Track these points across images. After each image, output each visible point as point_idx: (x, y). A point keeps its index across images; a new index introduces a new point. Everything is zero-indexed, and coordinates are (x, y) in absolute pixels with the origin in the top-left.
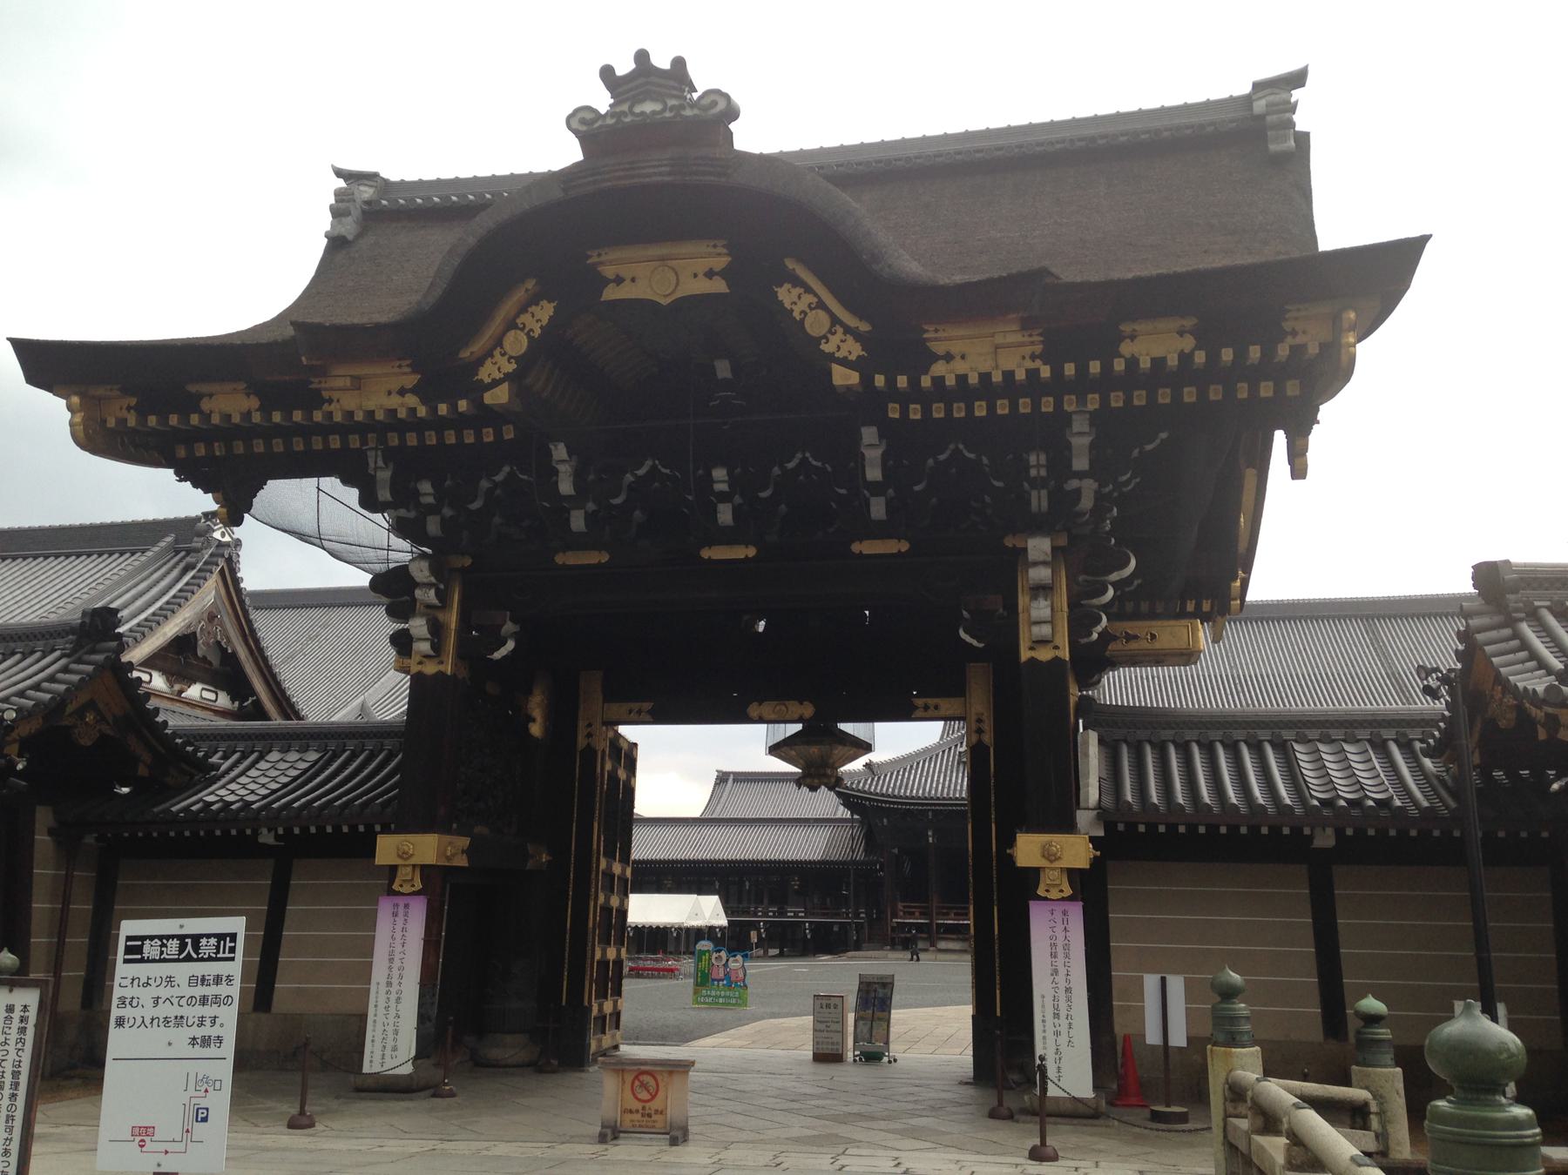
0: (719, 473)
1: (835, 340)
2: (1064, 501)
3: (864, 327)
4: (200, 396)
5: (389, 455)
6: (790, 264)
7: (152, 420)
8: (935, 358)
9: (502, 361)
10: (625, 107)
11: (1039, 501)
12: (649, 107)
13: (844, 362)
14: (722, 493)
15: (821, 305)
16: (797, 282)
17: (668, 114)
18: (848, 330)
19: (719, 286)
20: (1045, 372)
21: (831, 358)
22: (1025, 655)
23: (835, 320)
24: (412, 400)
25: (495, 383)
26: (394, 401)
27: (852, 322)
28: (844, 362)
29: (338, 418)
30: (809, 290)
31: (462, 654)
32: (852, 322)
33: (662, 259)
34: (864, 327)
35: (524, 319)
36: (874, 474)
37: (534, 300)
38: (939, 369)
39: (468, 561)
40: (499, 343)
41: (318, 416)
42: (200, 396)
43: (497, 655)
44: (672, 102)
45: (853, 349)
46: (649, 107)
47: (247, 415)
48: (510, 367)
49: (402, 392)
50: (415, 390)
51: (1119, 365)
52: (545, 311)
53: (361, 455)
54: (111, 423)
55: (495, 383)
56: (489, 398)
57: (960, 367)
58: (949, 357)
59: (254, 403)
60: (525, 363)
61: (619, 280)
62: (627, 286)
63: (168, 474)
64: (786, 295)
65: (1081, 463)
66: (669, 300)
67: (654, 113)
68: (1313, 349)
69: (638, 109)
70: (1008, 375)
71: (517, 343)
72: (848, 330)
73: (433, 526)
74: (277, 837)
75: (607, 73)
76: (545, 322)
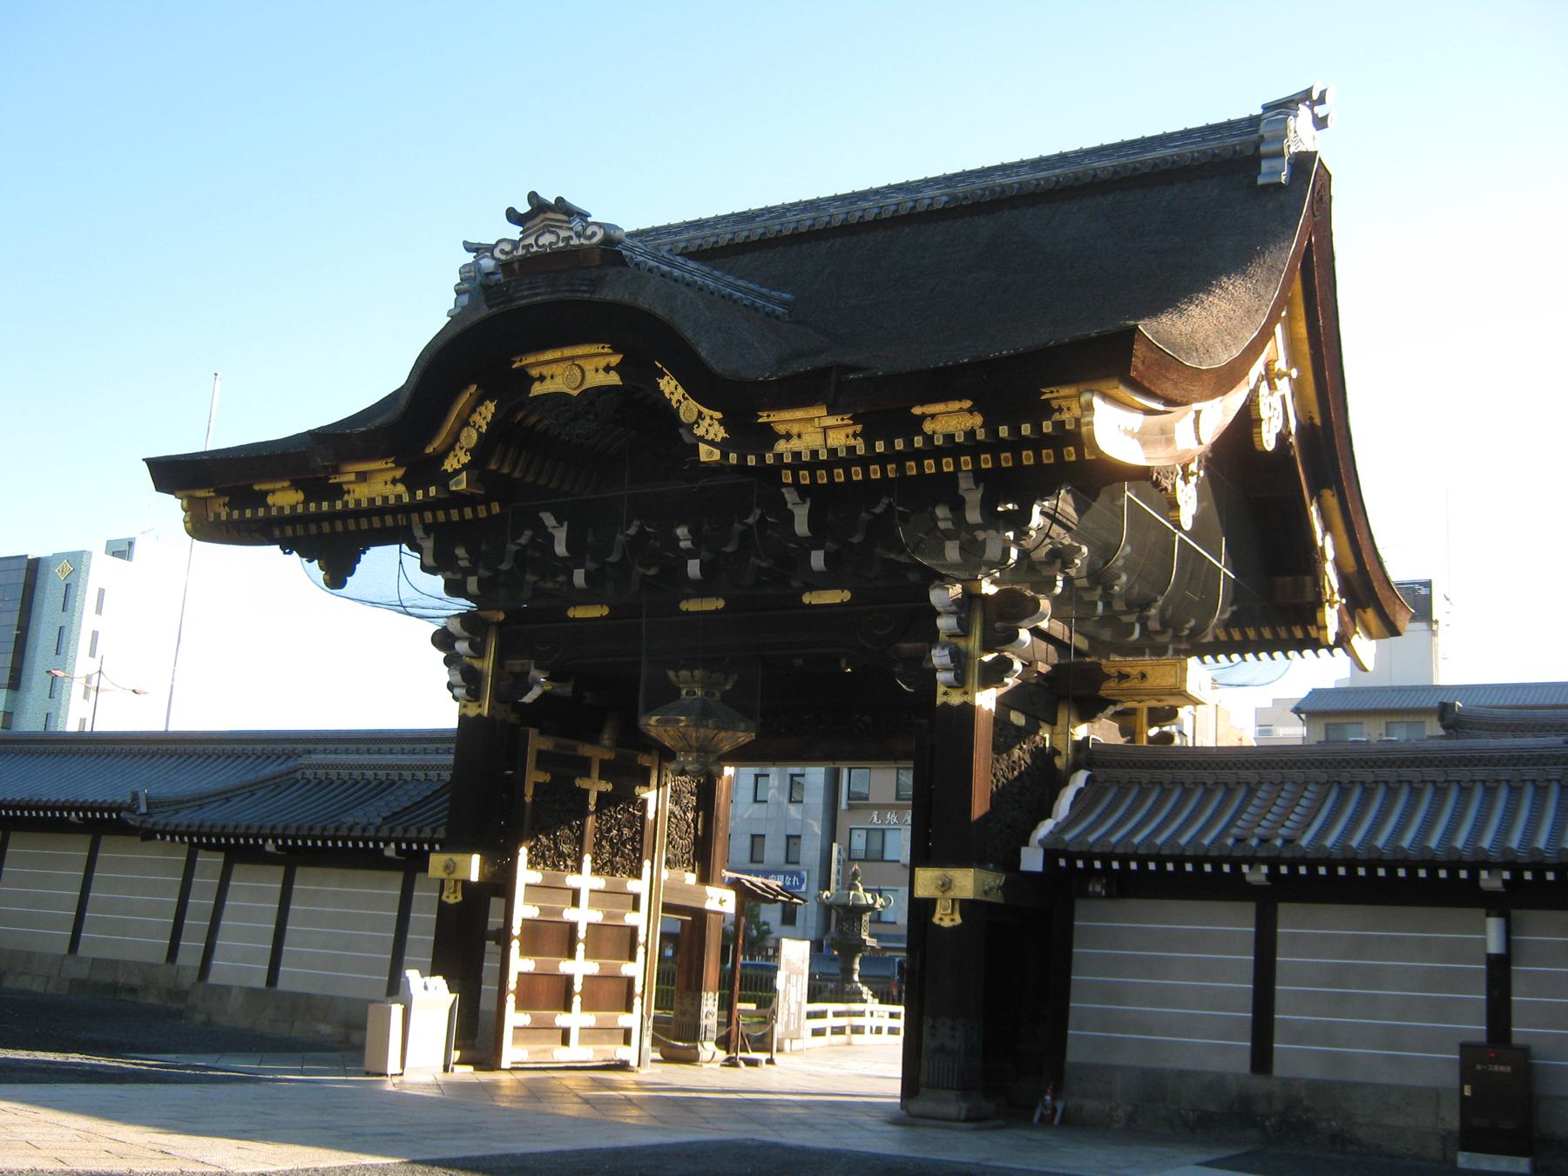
0: (682, 532)
4: (265, 494)
5: (428, 529)
7: (236, 514)
8: (777, 436)
9: (461, 454)
10: (531, 240)
12: (546, 239)
13: (712, 443)
14: (688, 550)
17: (561, 244)
19: (614, 379)
20: (861, 450)
21: (702, 439)
22: (940, 700)
24: (400, 488)
25: (457, 472)
28: (712, 443)
29: (352, 505)
31: (497, 697)
33: (572, 358)
35: (476, 417)
37: (479, 401)
38: (781, 446)
39: (501, 616)
40: (457, 439)
41: (339, 505)
42: (265, 494)
43: (529, 698)
44: (563, 234)
45: (719, 433)
46: (546, 239)
47: (294, 508)
48: (465, 459)
50: (403, 480)
51: (918, 442)
52: (489, 409)
53: (409, 528)
54: (212, 517)
59: (300, 496)
60: (480, 454)
61: (542, 378)
62: (548, 381)
63: (275, 549)
66: (575, 393)
67: (551, 244)
69: (541, 242)
70: (833, 452)
71: (470, 437)
73: (472, 584)
74: (278, 847)
75: (513, 216)
76: (489, 418)
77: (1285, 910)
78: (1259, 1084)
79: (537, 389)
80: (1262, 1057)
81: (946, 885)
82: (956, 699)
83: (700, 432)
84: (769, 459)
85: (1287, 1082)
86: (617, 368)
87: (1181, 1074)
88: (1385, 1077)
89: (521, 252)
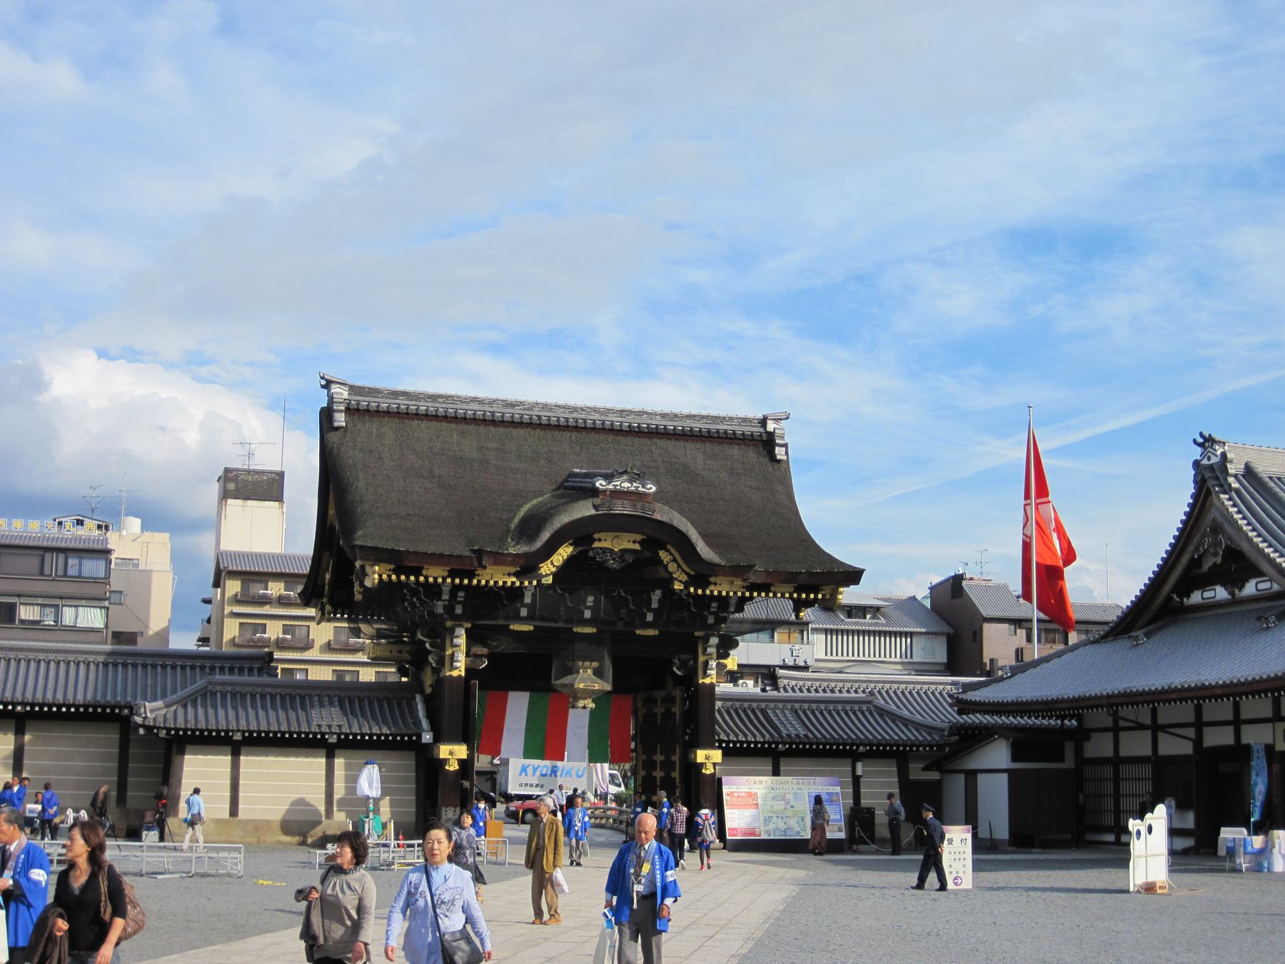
0: (591, 599)
11: (711, 620)
12: (626, 485)
16: (667, 550)
19: (637, 547)
25: (547, 575)
27: (688, 570)
32: (688, 570)
36: (655, 605)
38: (712, 587)
45: (685, 578)
49: (509, 575)
56: (544, 581)
58: (715, 584)
64: (662, 554)
79: (596, 544)
81: (707, 758)
82: (707, 681)
89: (610, 487)
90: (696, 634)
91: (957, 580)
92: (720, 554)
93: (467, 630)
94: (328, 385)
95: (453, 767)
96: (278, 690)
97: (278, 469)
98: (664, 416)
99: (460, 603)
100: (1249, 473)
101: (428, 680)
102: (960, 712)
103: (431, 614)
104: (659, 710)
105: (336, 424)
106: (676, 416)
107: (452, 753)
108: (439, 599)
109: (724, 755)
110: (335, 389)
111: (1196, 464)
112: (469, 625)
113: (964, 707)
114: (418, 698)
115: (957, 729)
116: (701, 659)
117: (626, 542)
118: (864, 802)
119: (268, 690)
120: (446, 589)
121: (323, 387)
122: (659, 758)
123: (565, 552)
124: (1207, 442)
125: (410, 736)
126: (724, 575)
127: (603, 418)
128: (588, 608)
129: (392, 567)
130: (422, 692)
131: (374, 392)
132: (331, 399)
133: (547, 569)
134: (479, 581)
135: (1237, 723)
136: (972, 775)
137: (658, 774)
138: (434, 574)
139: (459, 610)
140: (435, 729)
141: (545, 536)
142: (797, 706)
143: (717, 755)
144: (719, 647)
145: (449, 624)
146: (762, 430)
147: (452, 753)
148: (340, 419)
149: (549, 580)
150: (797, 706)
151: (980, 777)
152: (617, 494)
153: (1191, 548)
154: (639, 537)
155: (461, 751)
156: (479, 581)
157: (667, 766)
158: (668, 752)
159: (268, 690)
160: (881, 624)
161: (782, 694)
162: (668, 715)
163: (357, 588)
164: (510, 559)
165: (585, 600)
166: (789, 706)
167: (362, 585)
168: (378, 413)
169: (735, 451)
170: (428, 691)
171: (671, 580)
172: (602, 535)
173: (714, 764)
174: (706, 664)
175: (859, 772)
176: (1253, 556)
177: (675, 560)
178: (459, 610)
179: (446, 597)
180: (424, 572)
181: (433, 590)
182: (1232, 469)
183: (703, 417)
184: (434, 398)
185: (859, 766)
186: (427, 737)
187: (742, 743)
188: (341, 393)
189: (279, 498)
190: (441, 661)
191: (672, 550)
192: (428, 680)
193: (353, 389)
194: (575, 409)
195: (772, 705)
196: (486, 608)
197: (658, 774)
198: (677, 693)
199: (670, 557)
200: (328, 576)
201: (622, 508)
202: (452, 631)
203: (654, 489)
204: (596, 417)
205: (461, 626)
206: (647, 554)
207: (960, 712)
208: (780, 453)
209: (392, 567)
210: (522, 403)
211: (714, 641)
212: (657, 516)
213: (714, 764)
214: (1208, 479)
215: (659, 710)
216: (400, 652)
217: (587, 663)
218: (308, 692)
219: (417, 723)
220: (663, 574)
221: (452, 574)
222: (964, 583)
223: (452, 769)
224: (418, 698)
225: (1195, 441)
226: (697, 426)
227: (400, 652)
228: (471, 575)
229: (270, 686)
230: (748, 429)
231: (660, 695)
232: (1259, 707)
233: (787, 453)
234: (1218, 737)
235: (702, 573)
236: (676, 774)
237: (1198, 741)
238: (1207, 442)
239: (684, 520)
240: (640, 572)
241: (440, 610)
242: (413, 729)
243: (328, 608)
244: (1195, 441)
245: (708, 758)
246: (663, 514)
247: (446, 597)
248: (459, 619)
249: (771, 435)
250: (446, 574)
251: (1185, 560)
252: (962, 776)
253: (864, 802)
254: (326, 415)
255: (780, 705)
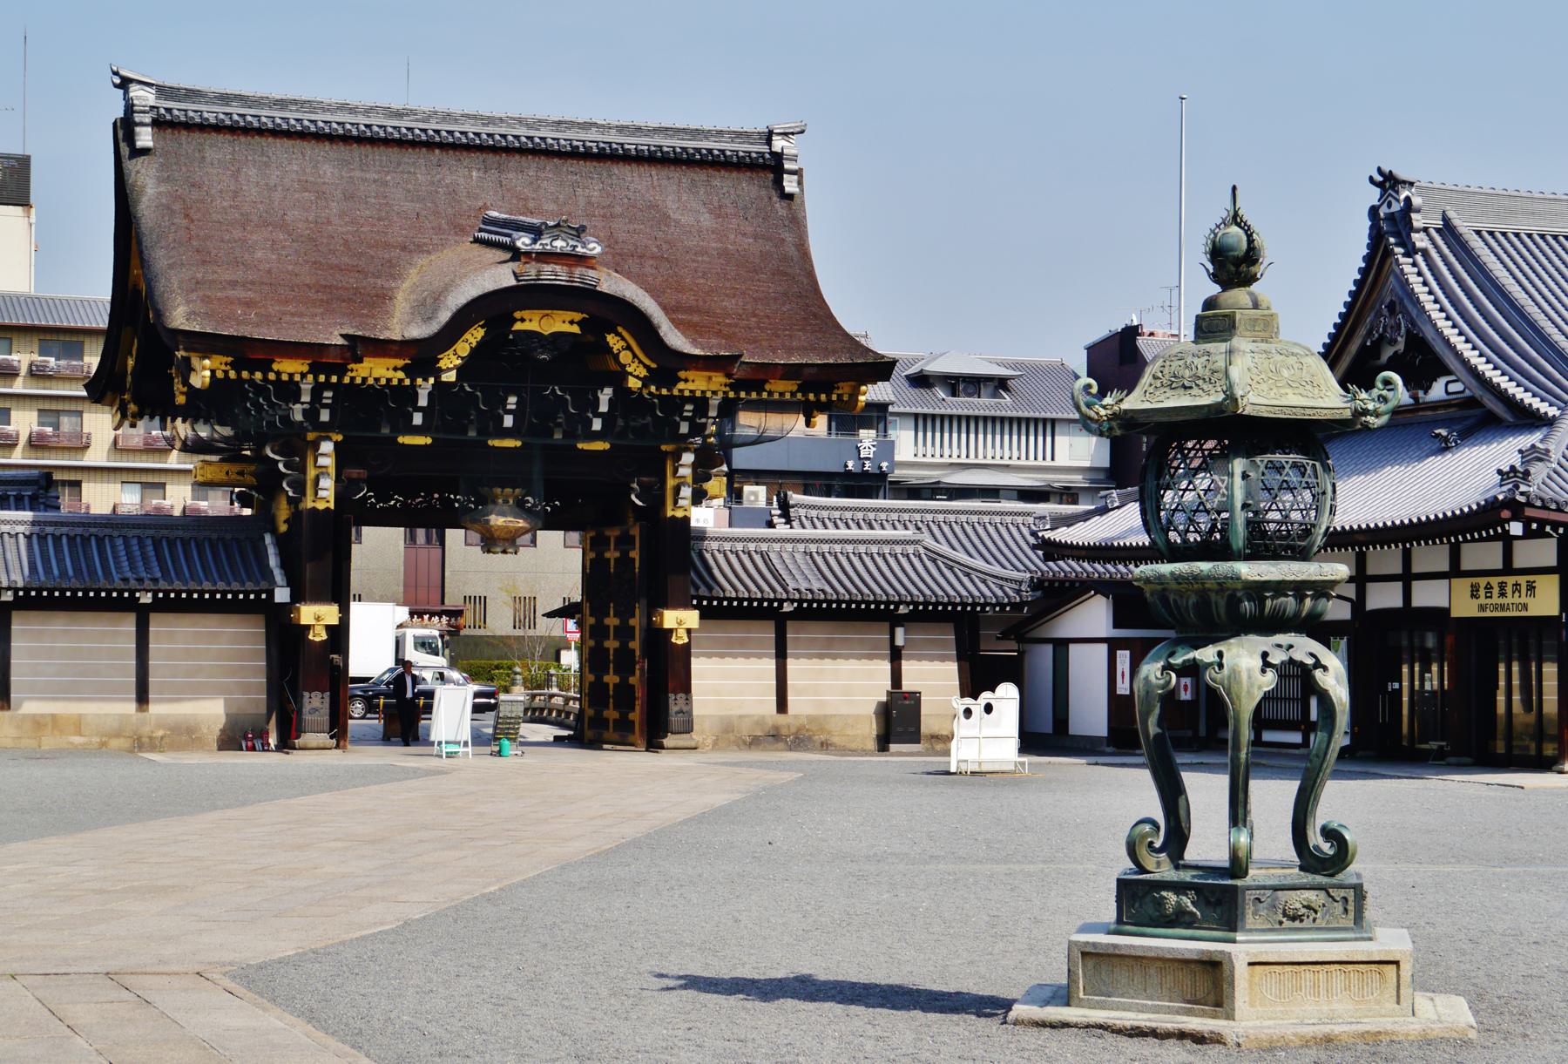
0: (512, 400)
1: (634, 366)
2: (697, 429)
3: (654, 366)
6: (620, 329)
8: (680, 380)
11: (684, 428)
12: (559, 244)
15: (629, 348)
16: (618, 334)
18: (640, 362)
19: (576, 329)
23: (635, 356)
24: (401, 375)
26: (390, 374)
27: (647, 362)
30: (623, 339)
32: (647, 362)
34: (654, 366)
36: (604, 408)
38: (681, 385)
45: (643, 372)
49: (395, 369)
55: (449, 370)
56: (445, 378)
57: (690, 386)
58: (686, 381)
61: (523, 320)
65: (713, 413)
68: (846, 398)
72: (640, 362)
77: (789, 623)
78: (782, 719)
80: (782, 705)
82: (679, 514)
83: (629, 369)
84: (676, 392)
85: (796, 716)
86: (578, 323)
87: (741, 717)
88: (844, 711)
89: (538, 247)
90: (664, 448)
91: (1131, 332)
92: (694, 343)
93: (336, 443)
94: (125, 83)
95: (319, 636)
96: (64, 530)
97: (17, 150)
98: (621, 129)
99: (326, 406)
100: (1448, 230)
101: (283, 512)
102: (1047, 558)
103: (286, 420)
104: (612, 555)
105: (139, 144)
106: (639, 129)
107: (316, 616)
108: (297, 401)
109: (702, 617)
110: (136, 92)
111: (1373, 211)
112: (340, 438)
113: (1053, 550)
114: (268, 539)
115: (1037, 584)
116: (671, 483)
117: (560, 323)
118: (907, 685)
119: (49, 529)
120: (306, 387)
121: (116, 86)
122: (612, 621)
123: (475, 335)
124: (1388, 183)
125: (258, 594)
126: (697, 369)
127: (531, 133)
128: (509, 412)
129: (230, 359)
130: (274, 531)
131: (192, 94)
132: (130, 108)
133: (450, 363)
134: (353, 379)
135: (1407, 578)
136: (1062, 645)
137: (612, 644)
138: (288, 367)
139: (325, 416)
140: (291, 582)
141: (444, 316)
142: (813, 548)
143: (691, 618)
144: (695, 466)
145: (311, 436)
146: (765, 149)
147: (316, 616)
148: (145, 138)
149: (451, 377)
150: (813, 548)
151: (1072, 647)
152: (546, 257)
153: (1362, 331)
154: (578, 316)
155: (330, 614)
156: (353, 379)
157: (625, 632)
158: (625, 613)
159: (49, 529)
160: (1005, 405)
161: (797, 531)
162: (625, 561)
163: (178, 387)
164: (396, 348)
165: (504, 403)
166: (801, 547)
167: (186, 382)
168: (203, 127)
169: (723, 182)
170: (283, 528)
171: (624, 374)
172: (526, 314)
173: (689, 631)
174: (677, 490)
175: (899, 641)
176: (1439, 347)
177: (629, 348)
178: (325, 416)
179: (306, 398)
180: (275, 367)
181: (289, 390)
182: (1418, 220)
183: (678, 130)
184: (282, 104)
185: (900, 632)
186: (282, 595)
187: (730, 600)
188: (144, 97)
189: (20, 198)
190: (300, 487)
191: (625, 334)
192: (283, 512)
193: (163, 91)
194: (490, 120)
195: (777, 546)
196: (364, 416)
197: (612, 644)
198: (635, 531)
199: (622, 343)
200: (131, 362)
201: (554, 274)
202: (315, 445)
203: (598, 249)
204: (522, 131)
205: (330, 439)
206: (590, 338)
207: (1047, 558)
208: (790, 185)
209: (230, 359)
210: (413, 112)
211: (688, 458)
212: (604, 287)
213: (689, 631)
214: (1390, 229)
215: (612, 555)
216: (241, 473)
217: (508, 490)
218: (108, 531)
219: (267, 574)
220: (613, 366)
221: (315, 369)
222: (1140, 341)
223: (317, 639)
224: (268, 539)
225: (1371, 179)
226: (667, 143)
227: (241, 473)
228: (342, 370)
229: (51, 524)
230: (743, 147)
231: (613, 533)
232: (1431, 557)
233: (800, 183)
234: (1385, 597)
235: (668, 364)
236: (635, 645)
237: (1358, 604)
238: (1388, 183)
239: (641, 292)
240: (582, 360)
241: (298, 417)
242: (264, 585)
243: (132, 407)
244: (1371, 179)
245: (679, 620)
246: (611, 283)
247: (306, 398)
248: (325, 430)
249: (778, 157)
250: (305, 369)
251: (1354, 347)
252: (1049, 648)
253: (907, 685)
254: (125, 128)
255: (789, 547)
